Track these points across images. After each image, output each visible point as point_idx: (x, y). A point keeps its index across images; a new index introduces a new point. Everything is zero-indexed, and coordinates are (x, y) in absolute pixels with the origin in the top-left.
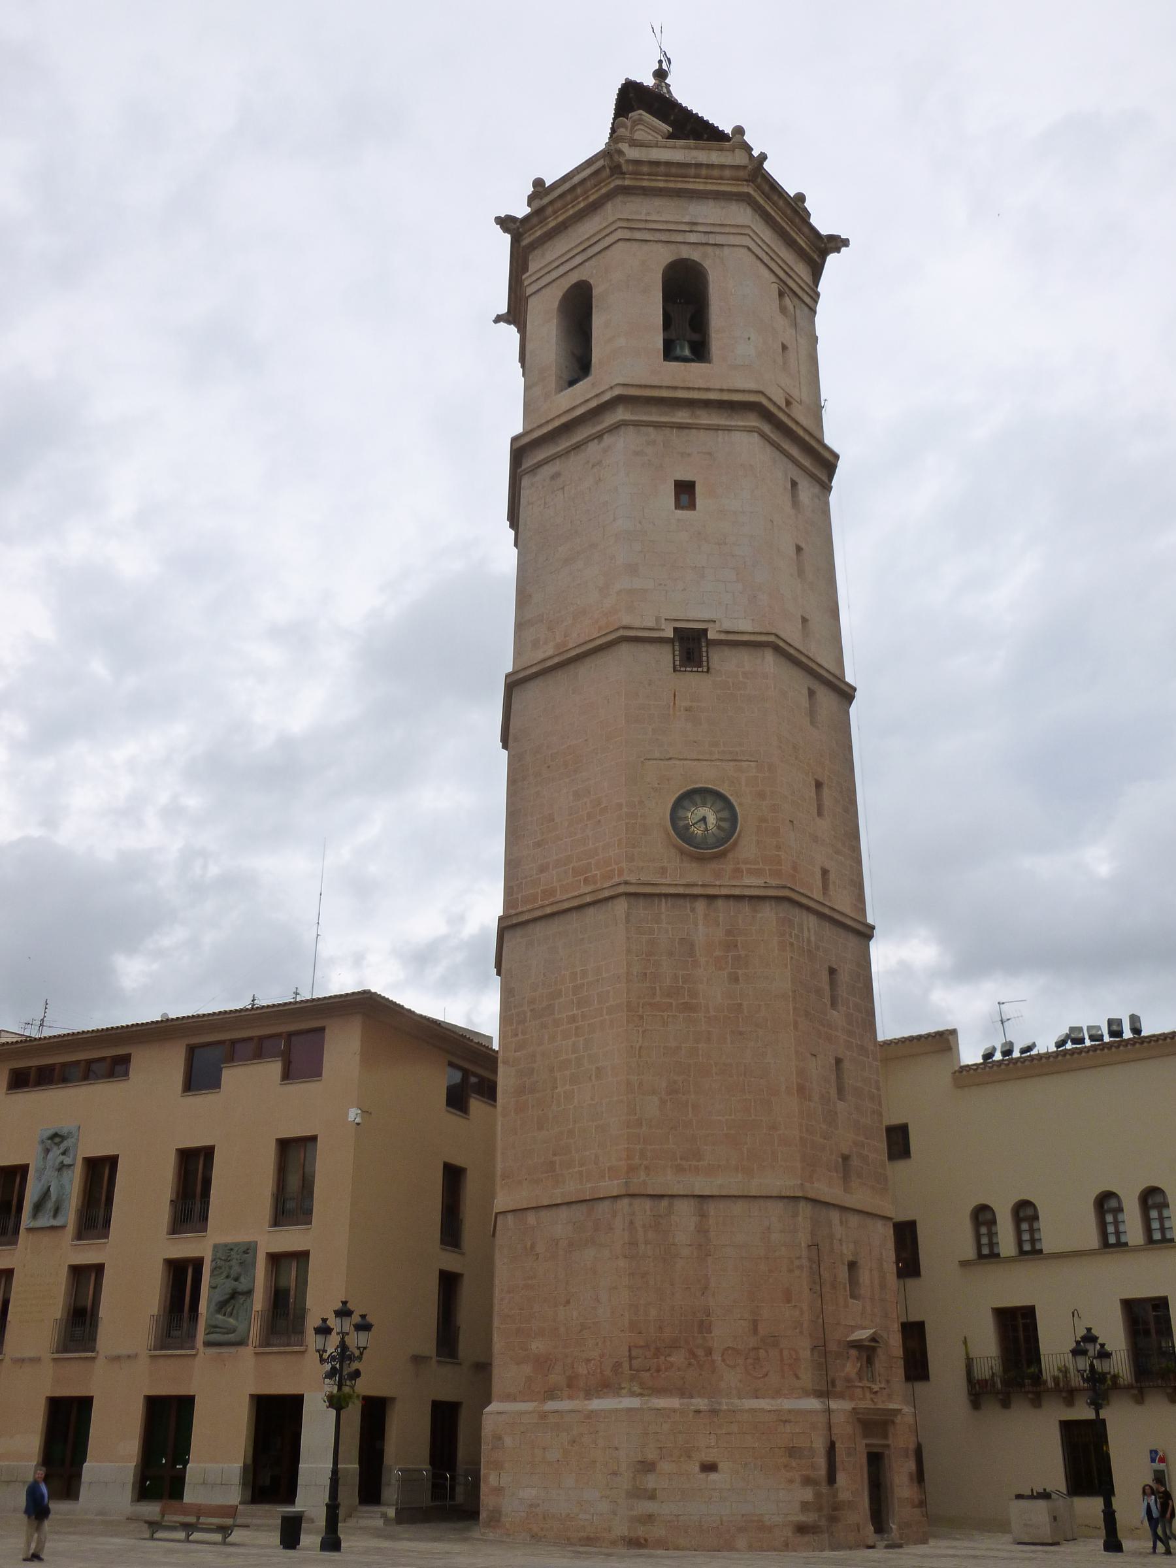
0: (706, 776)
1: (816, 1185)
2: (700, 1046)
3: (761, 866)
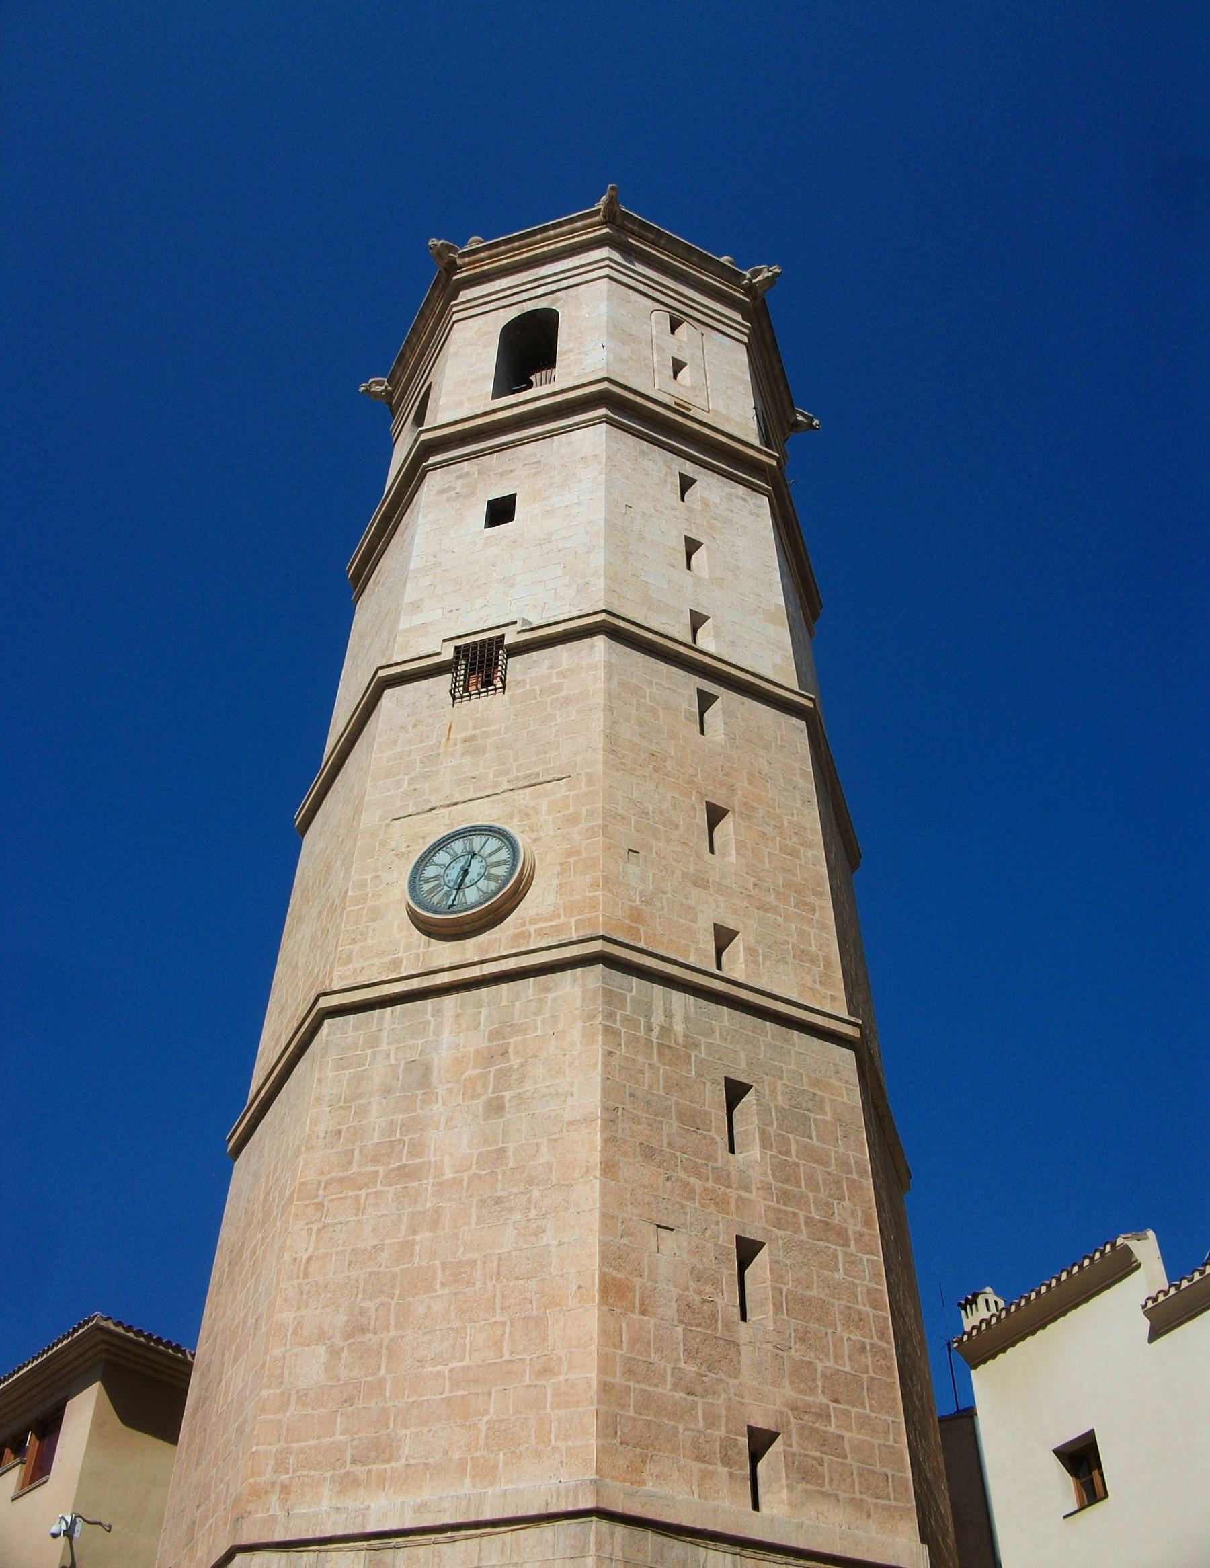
0: (482, 814)
1: (649, 1487)
2: (418, 1238)
3: (562, 920)
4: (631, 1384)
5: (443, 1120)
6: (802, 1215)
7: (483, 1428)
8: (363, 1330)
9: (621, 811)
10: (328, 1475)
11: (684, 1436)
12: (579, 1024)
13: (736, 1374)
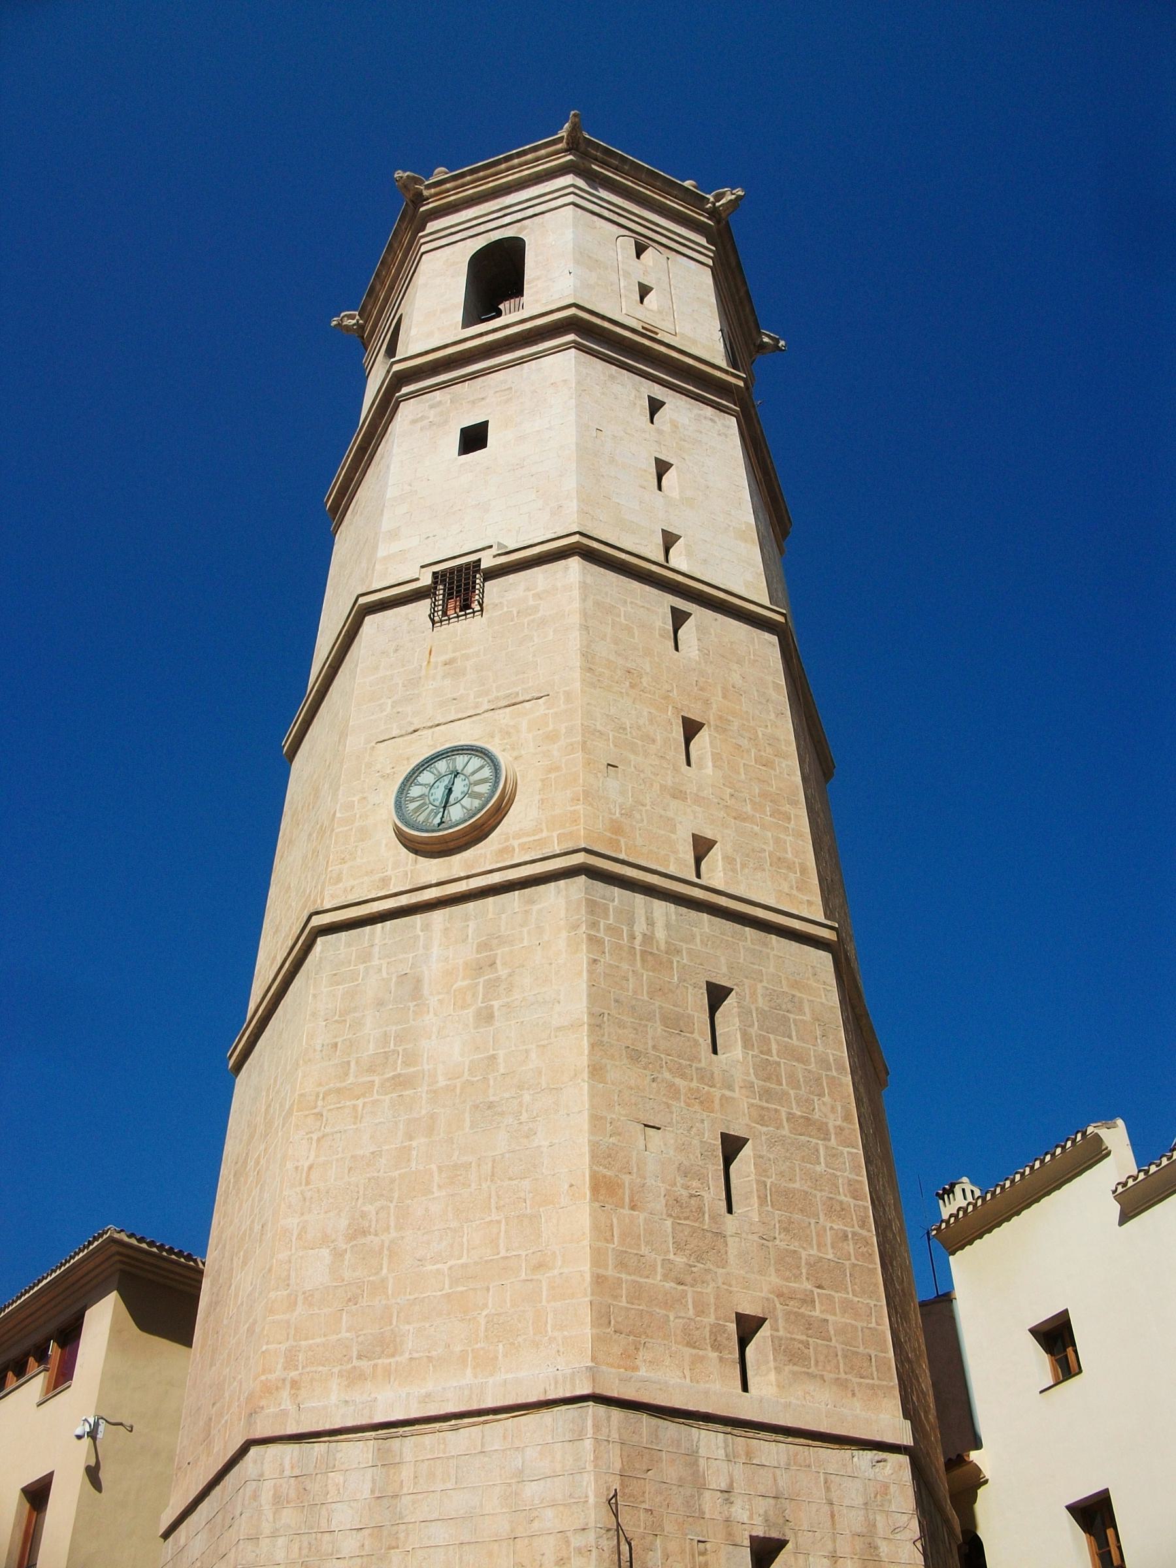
0: (465, 734)
1: (643, 1372)
2: (414, 1144)
3: (545, 834)
4: (623, 1276)
5: (435, 1029)
6: (783, 1111)
7: (482, 1321)
8: (365, 1233)
9: (599, 727)
10: (336, 1370)
11: (675, 1324)
12: (564, 934)
13: (724, 1263)
